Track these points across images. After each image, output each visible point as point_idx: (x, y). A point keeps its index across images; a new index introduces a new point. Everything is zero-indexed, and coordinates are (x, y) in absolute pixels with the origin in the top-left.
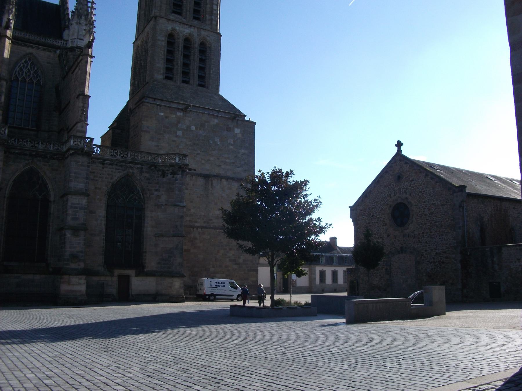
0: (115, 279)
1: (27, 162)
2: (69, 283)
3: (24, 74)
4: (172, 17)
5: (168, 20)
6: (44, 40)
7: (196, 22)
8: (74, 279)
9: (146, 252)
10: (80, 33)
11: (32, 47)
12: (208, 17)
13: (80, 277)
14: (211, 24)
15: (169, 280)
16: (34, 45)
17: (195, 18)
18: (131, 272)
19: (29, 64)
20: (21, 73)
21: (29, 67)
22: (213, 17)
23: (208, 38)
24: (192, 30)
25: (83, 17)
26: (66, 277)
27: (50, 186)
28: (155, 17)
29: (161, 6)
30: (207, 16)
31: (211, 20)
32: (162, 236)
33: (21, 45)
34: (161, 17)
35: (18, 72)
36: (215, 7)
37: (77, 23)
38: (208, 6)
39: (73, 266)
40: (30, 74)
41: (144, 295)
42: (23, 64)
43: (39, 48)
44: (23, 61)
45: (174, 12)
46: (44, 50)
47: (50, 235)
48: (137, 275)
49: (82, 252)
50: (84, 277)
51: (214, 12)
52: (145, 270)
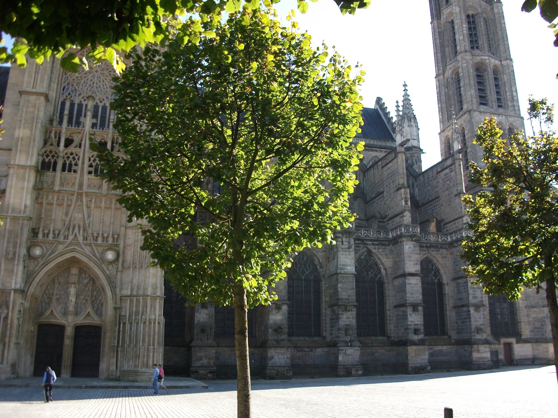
0: (502, 346)
1: (424, 253)
2: (478, 351)
4: (482, 108)
5: (480, 112)
6: (384, 144)
7: (501, 110)
8: (482, 348)
9: (520, 322)
10: (413, 134)
11: (377, 151)
12: (510, 104)
13: (485, 346)
14: (514, 110)
15: (544, 345)
17: (499, 106)
18: (513, 340)
22: (515, 104)
23: (515, 123)
24: (500, 118)
25: (412, 120)
26: (476, 346)
27: (442, 271)
28: (470, 112)
29: (472, 101)
30: (509, 102)
31: (514, 106)
32: (533, 307)
34: (475, 111)
36: (514, 94)
37: (408, 126)
38: (508, 93)
39: (478, 337)
41: (524, 359)
43: (381, 151)
45: (481, 104)
47: (448, 312)
48: (518, 342)
49: (483, 325)
50: (488, 346)
51: (515, 98)
52: (523, 337)
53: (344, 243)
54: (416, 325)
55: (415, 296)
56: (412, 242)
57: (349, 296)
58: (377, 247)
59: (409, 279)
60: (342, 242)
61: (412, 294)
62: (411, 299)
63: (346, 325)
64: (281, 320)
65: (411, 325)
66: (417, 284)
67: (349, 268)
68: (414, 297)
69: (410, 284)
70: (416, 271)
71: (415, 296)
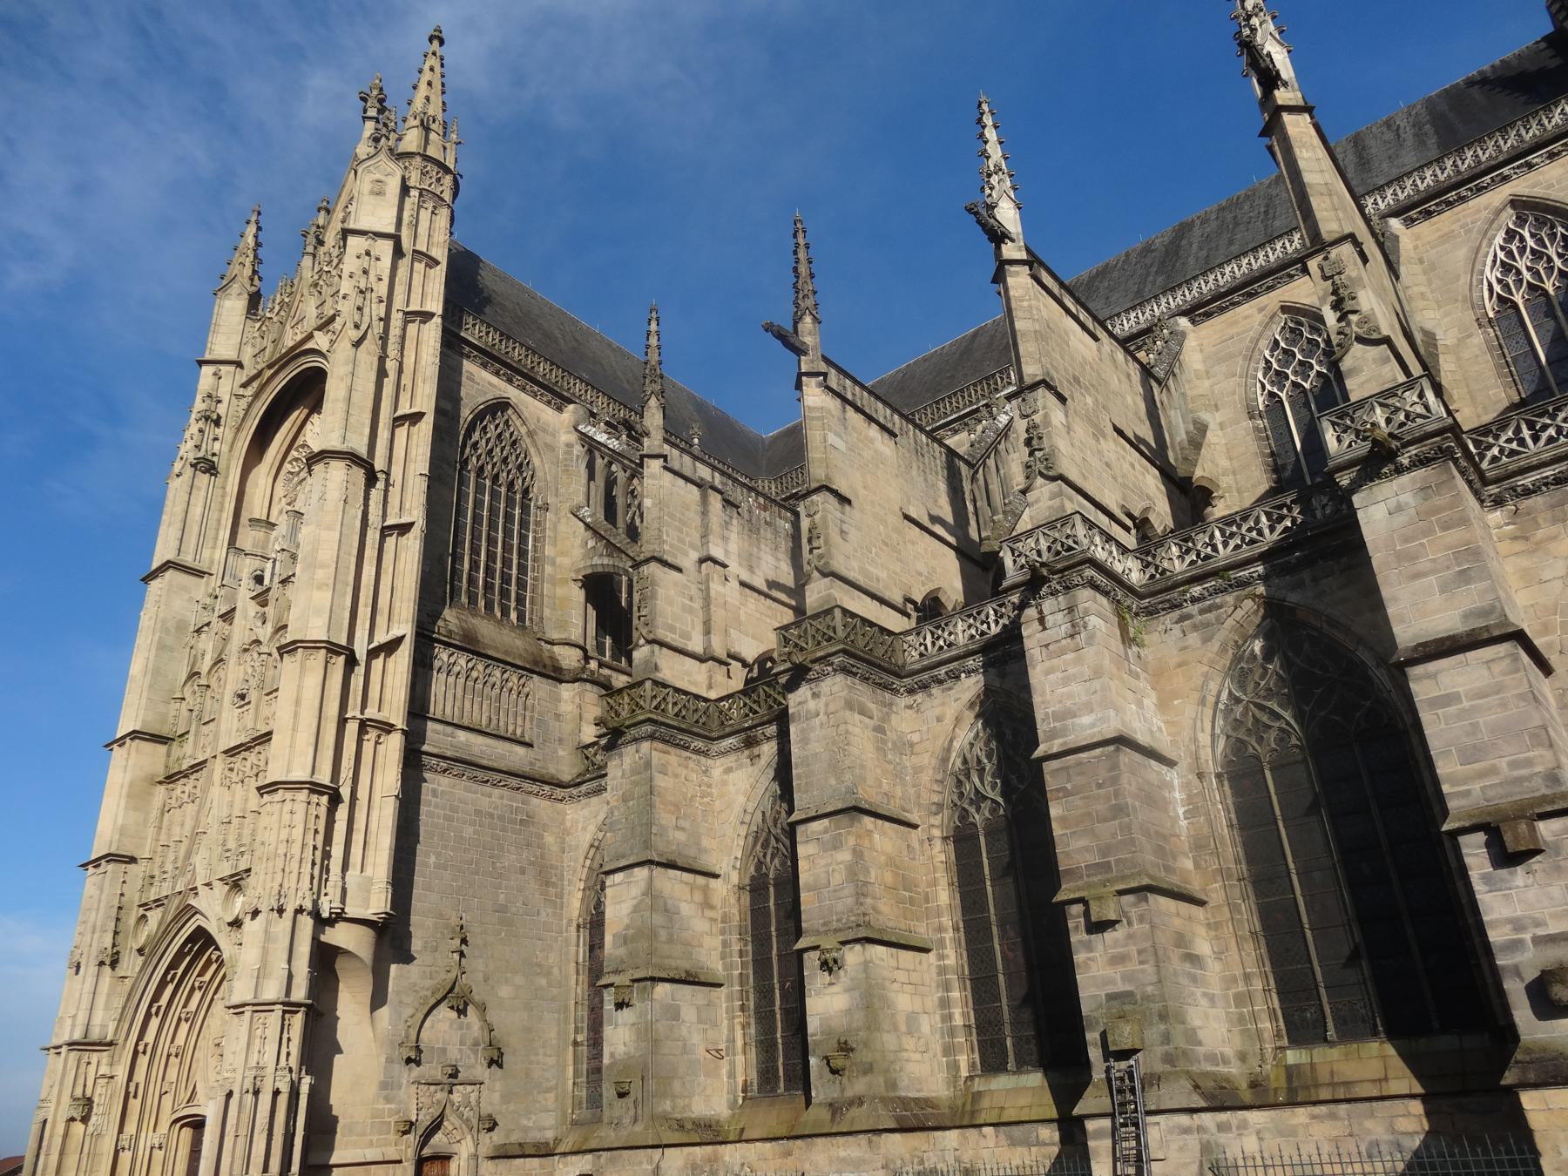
3: (1527, 276)
16: (1506, 171)
19: (1527, 235)
20: (1510, 280)
21: (1530, 242)
33: (1462, 199)
35: (1499, 281)
40: (1550, 260)
42: (1502, 248)
43: (1530, 166)
44: (1499, 240)
46: (1552, 156)
53: (1050, 620)
54: (1552, 939)
55: (1503, 764)
56: (1405, 478)
57: (1105, 850)
58: (1306, 575)
59: (1433, 676)
60: (1042, 620)
61: (1468, 756)
62: (1476, 787)
63: (1111, 997)
64: (848, 1011)
65: (1515, 945)
66: (1499, 689)
67: (1086, 720)
68: (1494, 771)
69: (1450, 699)
70: (1466, 616)
71: (1503, 764)
